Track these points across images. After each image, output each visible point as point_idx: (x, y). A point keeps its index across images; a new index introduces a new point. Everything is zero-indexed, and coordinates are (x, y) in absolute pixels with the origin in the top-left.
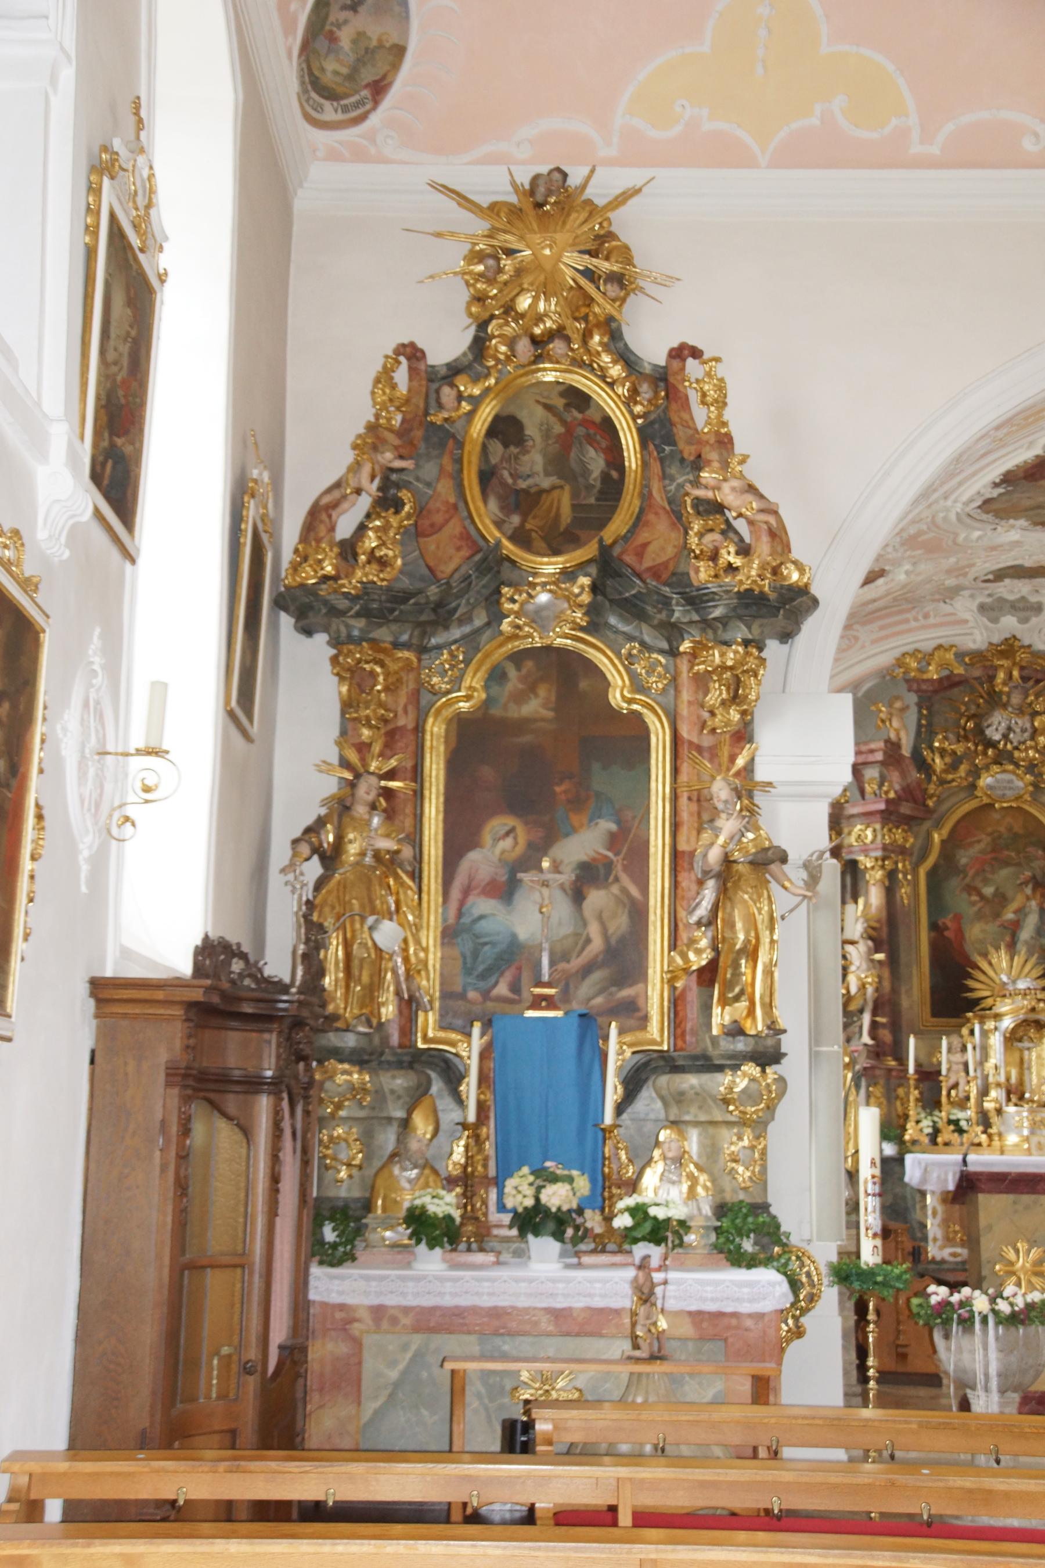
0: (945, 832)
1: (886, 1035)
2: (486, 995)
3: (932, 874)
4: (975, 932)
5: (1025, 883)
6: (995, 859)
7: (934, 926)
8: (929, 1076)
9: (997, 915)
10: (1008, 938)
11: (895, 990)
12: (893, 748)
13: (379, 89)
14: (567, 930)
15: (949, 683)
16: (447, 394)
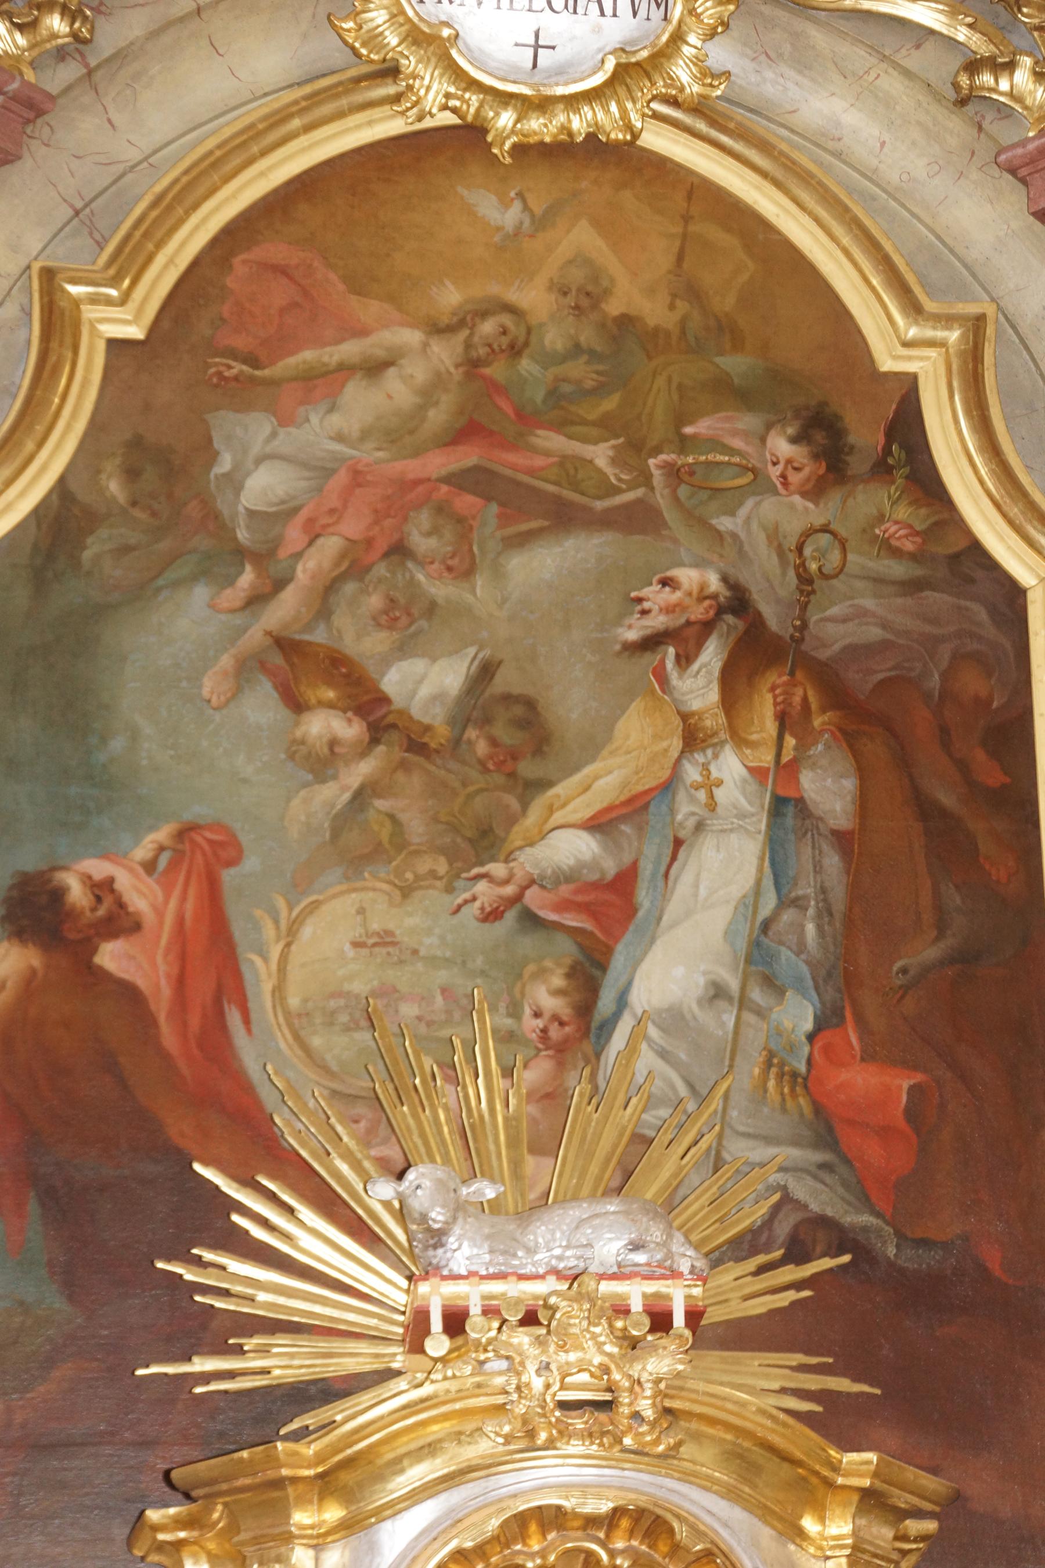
4: (319, 952)
5: (683, 639)
6: (476, 481)
9: (484, 841)
10: (547, 996)
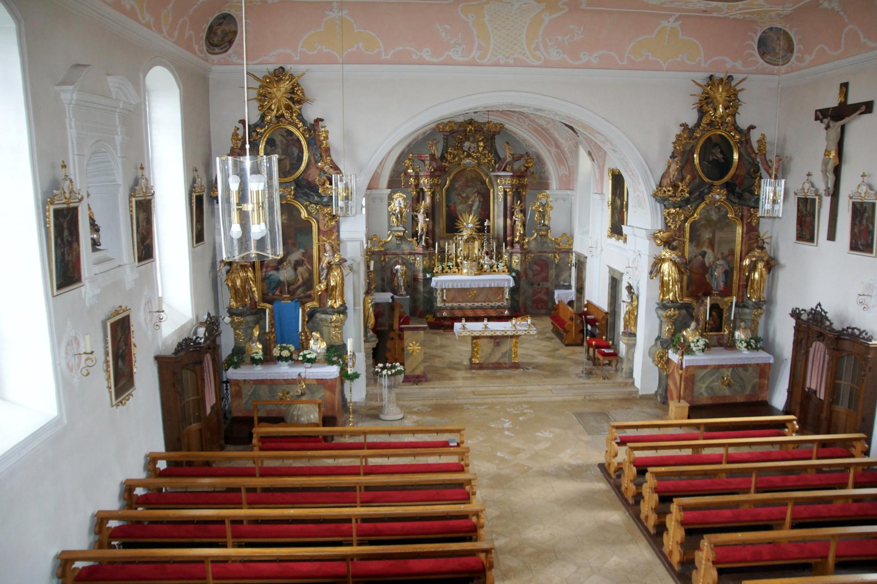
0: (451, 177)
1: (430, 241)
2: (273, 294)
3: (447, 190)
4: (460, 208)
7: (447, 206)
8: (442, 251)
9: (466, 202)
11: (434, 227)
12: (432, 156)
13: (231, 43)
14: (293, 277)
15: (452, 132)
16: (254, 134)
